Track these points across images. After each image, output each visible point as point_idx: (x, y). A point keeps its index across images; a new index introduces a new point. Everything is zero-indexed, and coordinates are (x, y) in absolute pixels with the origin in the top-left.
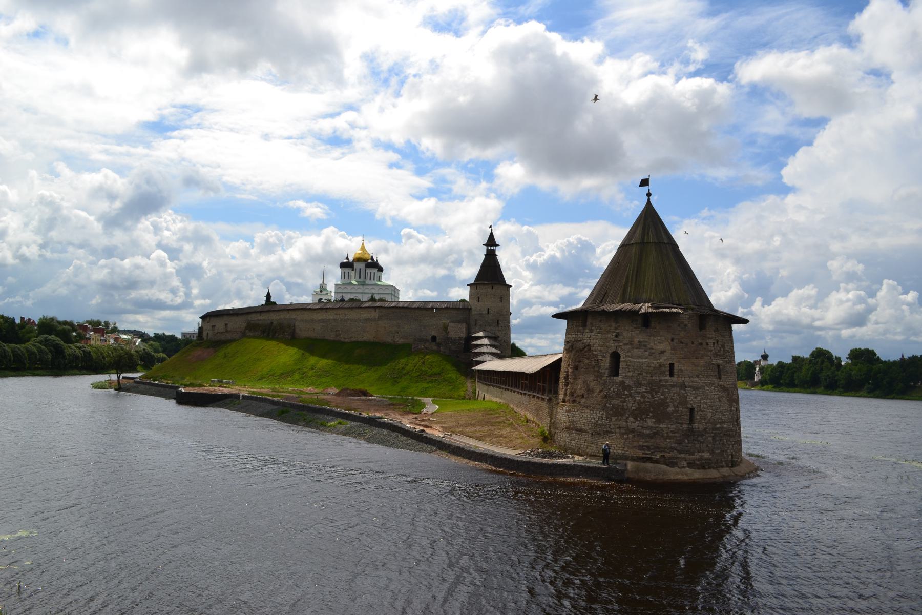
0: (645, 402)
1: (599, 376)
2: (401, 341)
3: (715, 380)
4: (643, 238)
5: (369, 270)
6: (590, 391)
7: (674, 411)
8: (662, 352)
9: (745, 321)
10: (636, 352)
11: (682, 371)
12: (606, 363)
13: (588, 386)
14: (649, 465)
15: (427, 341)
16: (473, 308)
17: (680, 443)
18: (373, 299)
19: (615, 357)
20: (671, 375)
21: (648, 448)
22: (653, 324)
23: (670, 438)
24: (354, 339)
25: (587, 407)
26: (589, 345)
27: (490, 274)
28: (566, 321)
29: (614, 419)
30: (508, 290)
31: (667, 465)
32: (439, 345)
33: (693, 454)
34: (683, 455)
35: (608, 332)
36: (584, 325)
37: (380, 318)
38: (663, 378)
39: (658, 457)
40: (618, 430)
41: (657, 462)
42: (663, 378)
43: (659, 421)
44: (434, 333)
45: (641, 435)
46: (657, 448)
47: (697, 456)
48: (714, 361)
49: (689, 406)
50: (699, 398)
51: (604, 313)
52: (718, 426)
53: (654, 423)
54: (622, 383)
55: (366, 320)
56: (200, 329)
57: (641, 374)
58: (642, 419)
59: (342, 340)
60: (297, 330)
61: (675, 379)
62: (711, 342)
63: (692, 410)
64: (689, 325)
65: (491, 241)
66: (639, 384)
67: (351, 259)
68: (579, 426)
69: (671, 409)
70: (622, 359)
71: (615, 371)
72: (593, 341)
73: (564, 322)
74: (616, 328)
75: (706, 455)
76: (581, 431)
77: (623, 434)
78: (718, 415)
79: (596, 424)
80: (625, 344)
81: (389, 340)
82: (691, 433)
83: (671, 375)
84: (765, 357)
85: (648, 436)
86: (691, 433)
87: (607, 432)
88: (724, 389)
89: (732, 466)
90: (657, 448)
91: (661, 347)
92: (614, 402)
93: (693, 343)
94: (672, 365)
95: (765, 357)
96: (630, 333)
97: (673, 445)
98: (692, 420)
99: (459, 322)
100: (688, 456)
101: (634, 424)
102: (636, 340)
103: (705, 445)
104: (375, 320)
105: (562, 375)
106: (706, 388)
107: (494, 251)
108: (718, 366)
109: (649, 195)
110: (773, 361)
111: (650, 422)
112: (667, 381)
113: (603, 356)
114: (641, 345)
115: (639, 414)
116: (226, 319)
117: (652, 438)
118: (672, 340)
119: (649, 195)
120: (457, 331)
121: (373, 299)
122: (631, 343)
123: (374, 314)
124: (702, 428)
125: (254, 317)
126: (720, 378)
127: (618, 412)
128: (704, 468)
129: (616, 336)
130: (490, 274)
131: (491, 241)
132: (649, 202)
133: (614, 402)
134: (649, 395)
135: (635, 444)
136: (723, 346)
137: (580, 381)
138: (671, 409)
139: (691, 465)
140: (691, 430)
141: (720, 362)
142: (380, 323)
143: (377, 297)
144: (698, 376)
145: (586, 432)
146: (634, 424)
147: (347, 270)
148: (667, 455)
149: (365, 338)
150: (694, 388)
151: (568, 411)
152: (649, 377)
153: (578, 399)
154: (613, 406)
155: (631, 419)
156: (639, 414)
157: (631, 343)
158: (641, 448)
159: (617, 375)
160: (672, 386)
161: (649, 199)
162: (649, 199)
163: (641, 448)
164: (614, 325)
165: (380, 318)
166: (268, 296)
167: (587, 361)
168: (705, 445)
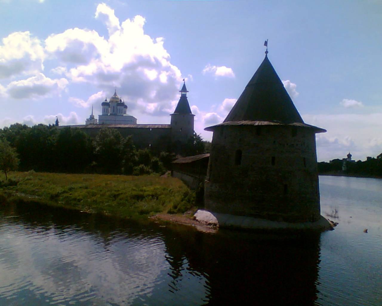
5: (118, 107)
19: (239, 153)
30: (193, 118)
67: (108, 101)
70: (243, 154)
93: (287, 144)
94: (273, 159)
107: (186, 95)
108: (304, 158)
109: (267, 52)
119: (267, 52)
132: (266, 58)
147: (106, 107)
161: (266, 56)
162: (266, 56)
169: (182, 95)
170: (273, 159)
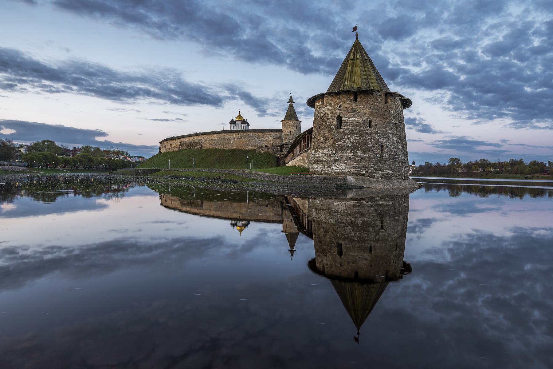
0: (356, 142)
1: (331, 129)
2: (251, 148)
4: (354, 57)
5: (243, 125)
6: (326, 139)
7: (372, 147)
8: (365, 114)
11: (376, 125)
12: (334, 122)
13: (325, 136)
17: (376, 164)
19: (340, 118)
20: (370, 127)
21: (359, 167)
22: (359, 99)
23: (369, 161)
25: (325, 148)
29: (339, 152)
32: (268, 149)
37: (241, 137)
43: (364, 153)
45: (354, 161)
47: (385, 172)
48: (393, 121)
50: (386, 140)
53: (361, 154)
54: (343, 132)
58: (355, 152)
61: (372, 129)
63: (382, 146)
64: (380, 100)
66: (352, 132)
69: (370, 146)
70: (343, 119)
71: (339, 126)
74: (339, 103)
75: (391, 172)
76: (322, 161)
77: (345, 160)
79: (330, 157)
82: (381, 159)
83: (370, 127)
86: (381, 159)
87: (336, 160)
90: (363, 168)
91: (364, 111)
92: (340, 143)
94: (370, 122)
101: (350, 154)
103: (389, 166)
111: (359, 153)
112: (367, 130)
113: (333, 119)
114: (353, 111)
115: (353, 149)
117: (360, 162)
122: (348, 110)
124: (388, 156)
127: (341, 148)
128: (389, 179)
129: (340, 107)
133: (340, 143)
135: (351, 166)
141: (397, 122)
142: (241, 140)
148: (370, 171)
150: (382, 134)
153: (320, 145)
156: (353, 149)
160: (370, 133)
165: (241, 137)
168: (389, 166)
170: (370, 122)
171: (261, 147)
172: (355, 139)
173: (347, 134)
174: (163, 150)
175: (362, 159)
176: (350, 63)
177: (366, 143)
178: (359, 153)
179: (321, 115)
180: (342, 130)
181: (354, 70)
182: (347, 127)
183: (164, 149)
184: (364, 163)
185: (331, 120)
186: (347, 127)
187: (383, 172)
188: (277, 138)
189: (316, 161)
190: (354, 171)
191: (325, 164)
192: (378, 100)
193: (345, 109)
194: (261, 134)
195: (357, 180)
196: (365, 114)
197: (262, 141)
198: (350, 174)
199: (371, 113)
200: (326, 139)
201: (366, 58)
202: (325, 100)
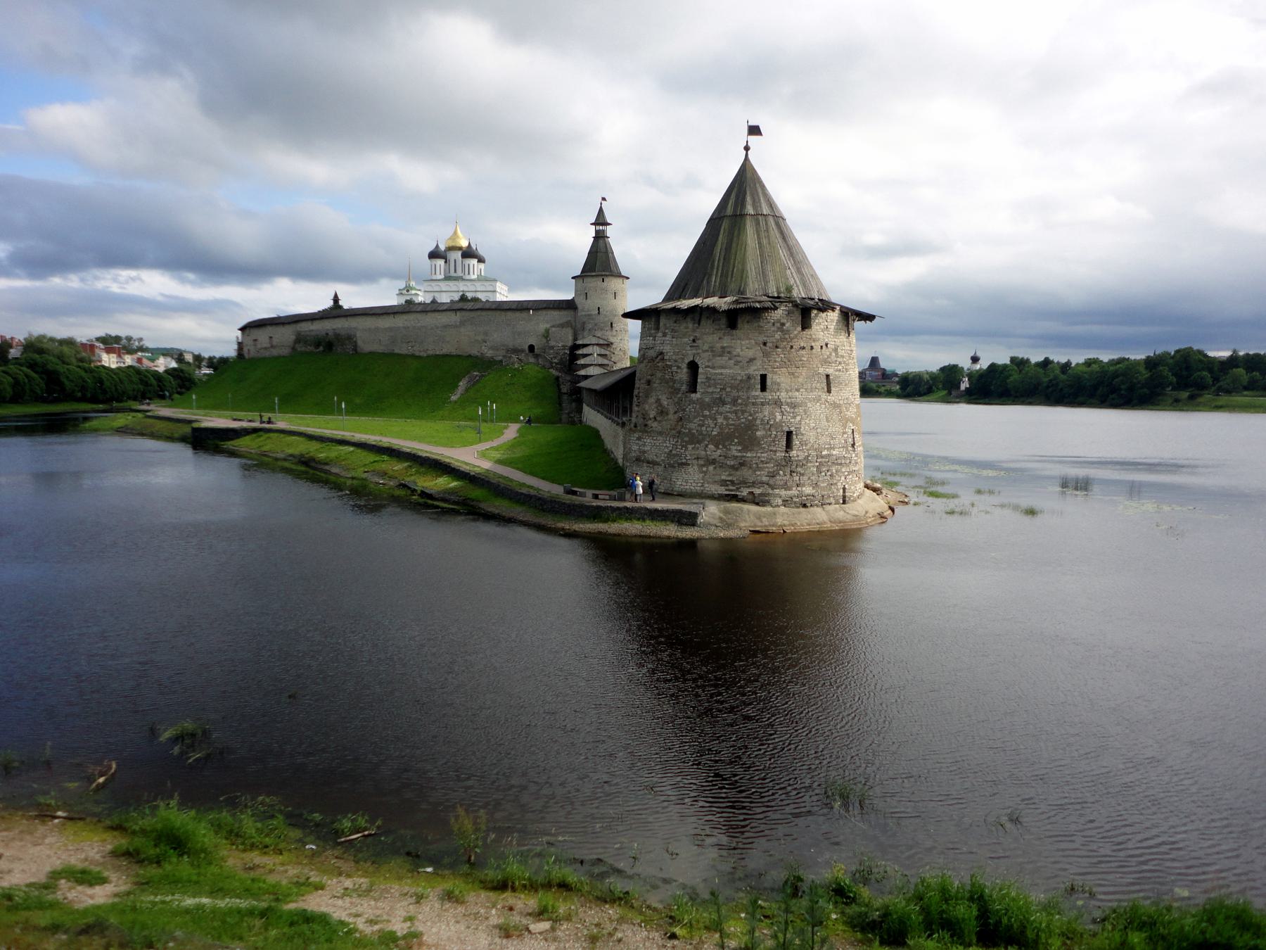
2: (489, 353)
3: (824, 396)
4: (735, 209)
6: (663, 412)
7: (764, 437)
8: (751, 360)
9: (869, 318)
10: (719, 361)
11: (779, 384)
12: (683, 374)
13: (661, 405)
14: (735, 505)
15: (523, 351)
16: (580, 307)
18: (463, 298)
19: (693, 367)
20: (763, 388)
21: (732, 482)
23: (759, 469)
24: (430, 353)
25: (660, 433)
26: (662, 353)
27: (600, 262)
28: (640, 322)
29: (690, 447)
31: (757, 504)
32: (537, 356)
33: (790, 489)
34: (777, 491)
35: (684, 335)
36: (658, 329)
37: (462, 323)
38: (754, 393)
39: (745, 493)
40: (695, 462)
41: (743, 500)
42: (754, 393)
43: (745, 449)
44: (532, 341)
46: (744, 483)
47: (794, 492)
48: (821, 370)
49: (786, 429)
50: (798, 418)
51: (675, 311)
52: (825, 453)
55: (445, 327)
56: (240, 345)
57: (724, 389)
58: (724, 446)
59: (417, 354)
60: (360, 343)
61: (768, 395)
62: (817, 345)
63: (789, 434)
65: (600, 221)
67: (442, 248)
68: (651, 457)
70: (700, 370)
71: (693, 387)
72: (667, 348)
73: (635, 326)
74: (694, 331)
75: (808, 490)
76: (654, 463)
78: (823, 440)
79: (670, 454)
80: (705, 351)
81: (474, 352)
83: (763, 388)
84: (975, 359)
85: (732, 467)
88: (836, 406)
89: (844, 502)
90: (744, 483)
91: (750, 353)
94: (764, 377)
95: (975, 359)
96: (711, 337)
97: (765, 479)
98: (789, 445)
99: (562, 326)
100: (783, 493)
101: (714, 452)
102: (718, 345)
104: (456, 326)
105: (636, 392)
106: (809, 405)
108: (828, 376)
109: (747, 148)
110: (983, 364)
111: (735, 450)
115: (722, 440)
116: (269, 330)
117: (737, 469)
118: (765, 344)
119: (747, 148)
120: (563, 339)
121: (463, 298)
122: (712, 349)
123: (454, 318)
124: (802, 456)
125: (305, 327)
126: (829, 391)
127: (695, 439)
128: (805, 506)
130: (600, 262)
131: (600, 221)
134: (732, 416)
135: (717, 478)
136: (836, 350)
137: (652, 400)
138: (758, 433)
139: (786, 503)
140: (788, 460)
141: (830, 371)
142: (462, 330)
143: (470, 295)
144: (798, 390)
145: (659, 464)
146: (714, 452)
148: (757, 491)
149: (445, 351)
151: (639, 439)
152: (735, 393)
154: (690, 430)
155: (711, 447)
156: (722, 440)
157: (712, 349)
158: (724, 483)
159: (695, 391)
160: (763, 404)
163: (724, 483)
164: (690, 325)
165: (462, 323)
166: (336, 299)
167: (659, 374)
168: (805, 478)
169: (597, 232)
171: (516, 351)
172: (726, 418)
173: (709, 405)
174: (251, 351)
175: (742, 464)
176: (725, 224)
177: (751, 426)
178: (735, 450)
179: (652, 353)
180: (698, 395)
181: (734, 245)
182: (710, 390)
183: (252, 349)
184: (745, 473)
185: (674, 369)
186: (710, 390)
187: (789, 493)
188: (562, 326)
189: (638, 459)
190: (722, 490)
191: (660, 469)
192: (783, 324)
193: (706, 347)
194: (518, 314)
195: (727, 512)
196: (751, 360)
197: (519, 334)
198: (712, 497)
199: (766, 355)
200: (663, 412)
201: (766, 211)
202: (663, 321)
